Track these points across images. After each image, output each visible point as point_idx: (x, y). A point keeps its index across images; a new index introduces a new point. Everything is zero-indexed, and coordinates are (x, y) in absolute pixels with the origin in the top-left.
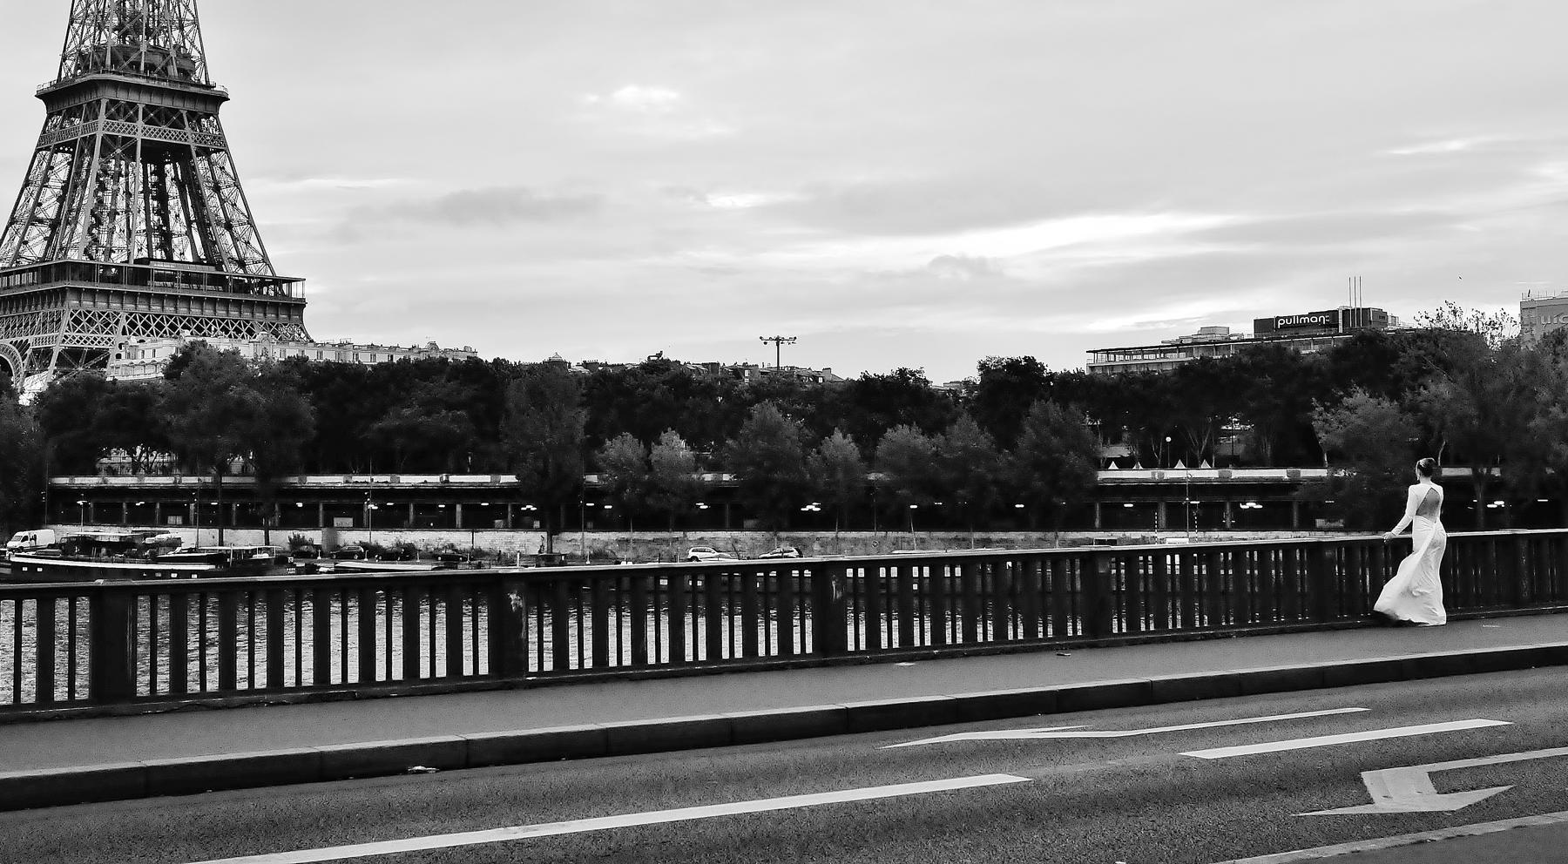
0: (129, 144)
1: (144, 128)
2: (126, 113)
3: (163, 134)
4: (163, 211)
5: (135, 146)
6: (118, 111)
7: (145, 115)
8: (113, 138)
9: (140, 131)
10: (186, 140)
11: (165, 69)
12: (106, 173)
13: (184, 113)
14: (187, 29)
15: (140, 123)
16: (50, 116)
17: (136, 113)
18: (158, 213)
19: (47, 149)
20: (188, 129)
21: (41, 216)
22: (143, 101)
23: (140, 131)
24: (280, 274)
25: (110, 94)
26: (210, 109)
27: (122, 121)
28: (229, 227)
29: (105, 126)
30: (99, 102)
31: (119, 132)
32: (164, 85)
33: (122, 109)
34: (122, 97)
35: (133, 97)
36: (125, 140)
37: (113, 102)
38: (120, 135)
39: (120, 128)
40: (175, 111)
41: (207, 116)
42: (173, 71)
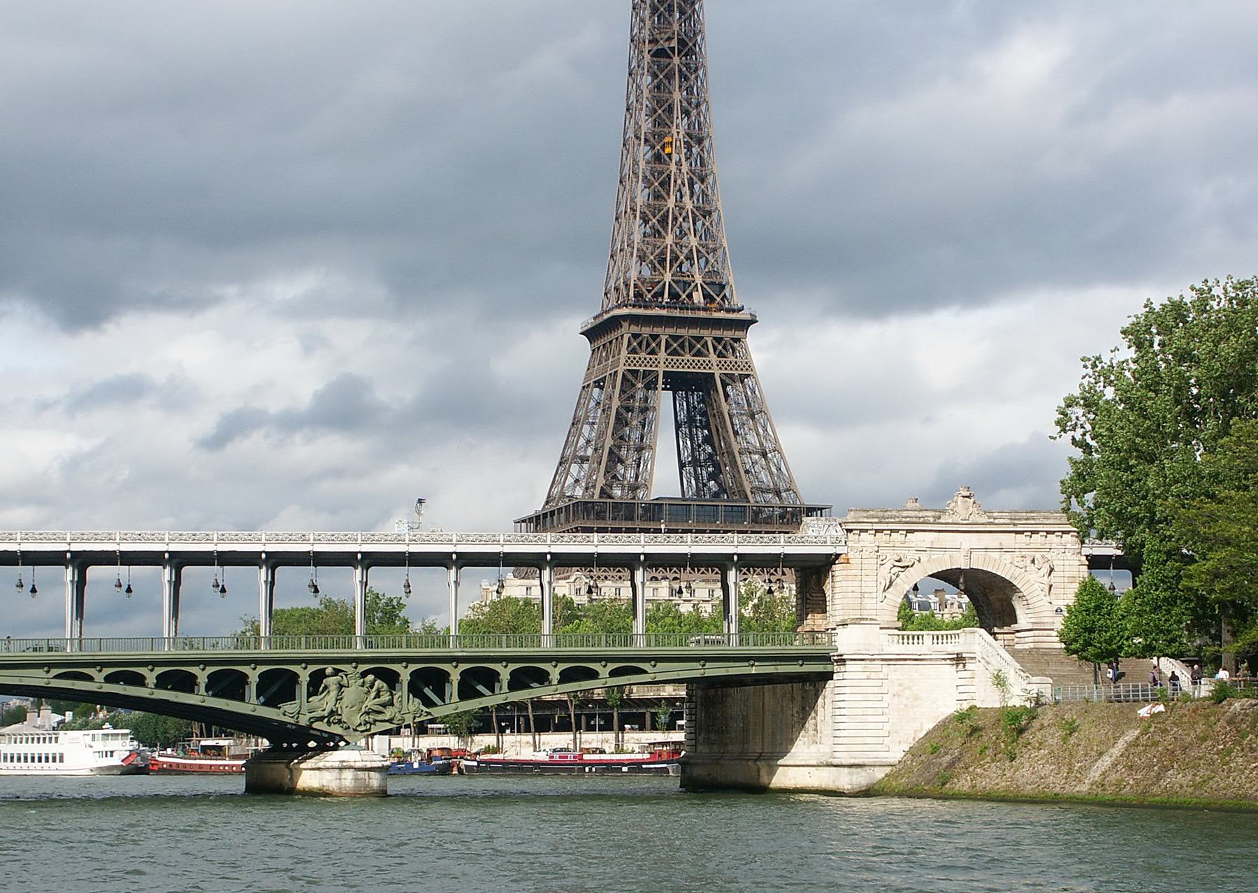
0: (650, 378)
1: (667, 360)
2: (648, 345)
3: (686, 364)
6: (640, 344)
7: (668, 346)
9: (662, 363)
10: (710, 368)
12: (628, 409)
15: (662, 355)
17: (659, 345)
20: (713, 357)
22: (664, 333)
23: (662, 363)
24: (809, 502)
26: (738, 334)
27: (643, 355)
29: (627, 361)
30: (622, 336)
31: (640, 365)
32: (690, 314)
33: (645, 343)
34: (646, 331)
35: (657, 331)
36: (646, 374)
37: (635, 336)
38: (642, 369)
39: (643, 362)
40: (699, 339)
41: (737, 340)
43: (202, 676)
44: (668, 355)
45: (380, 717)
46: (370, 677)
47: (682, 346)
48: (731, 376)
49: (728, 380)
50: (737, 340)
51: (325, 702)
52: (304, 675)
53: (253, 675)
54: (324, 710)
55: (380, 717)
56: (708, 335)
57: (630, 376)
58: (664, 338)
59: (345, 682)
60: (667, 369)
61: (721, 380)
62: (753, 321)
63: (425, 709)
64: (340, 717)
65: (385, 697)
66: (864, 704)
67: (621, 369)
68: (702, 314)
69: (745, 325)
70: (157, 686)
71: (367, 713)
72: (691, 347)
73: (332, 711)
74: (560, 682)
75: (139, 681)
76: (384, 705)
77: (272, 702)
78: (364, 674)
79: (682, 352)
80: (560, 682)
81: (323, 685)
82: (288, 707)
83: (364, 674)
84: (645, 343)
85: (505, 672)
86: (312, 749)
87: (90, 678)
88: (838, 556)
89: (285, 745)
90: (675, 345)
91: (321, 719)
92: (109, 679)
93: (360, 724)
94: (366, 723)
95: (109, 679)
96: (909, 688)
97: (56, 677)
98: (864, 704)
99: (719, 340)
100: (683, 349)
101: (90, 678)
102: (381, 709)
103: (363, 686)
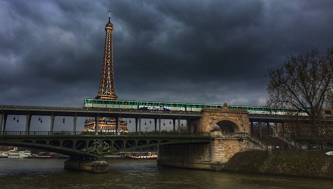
25: (102, 97)
32: (109, 96)
35: (105, 98)
42: (111, 94)
45: (107, 152)
52: (88, 142)
53: (75, 142)
55: (107, 152)
63: (117, 150)
65: (108, 147)
66: (219, 150)
68: (111, 96)
70: (49, 144)
71: (103, 151)
73: (95, 151)
74: (150, 143)
76: (108, 149)
77: (80, 148)
78: (103, 141)
80: (150, 143)
91: (92, 152)
92: (37, 142)
94: (103, 154)
96: (228, 146)
98: (219, 150)
101: (31, 142)
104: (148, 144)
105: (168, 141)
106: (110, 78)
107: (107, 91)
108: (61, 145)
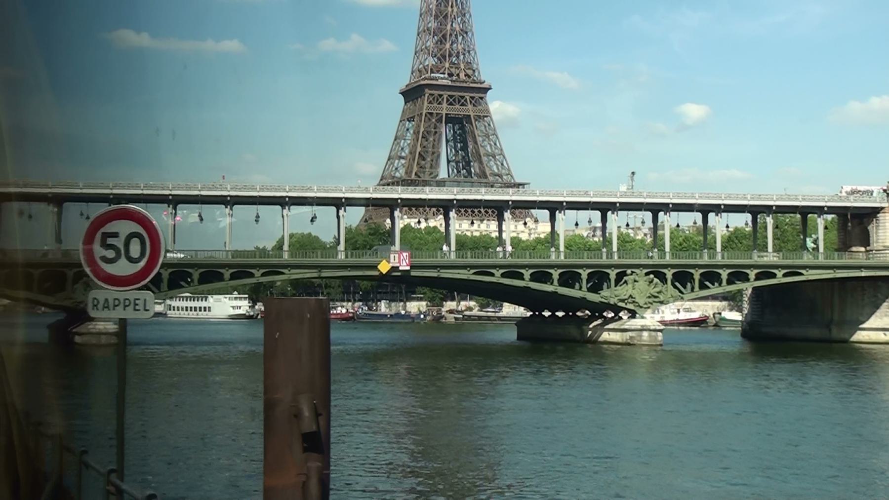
2: (438, 100)
3: (457, 110)
4: (465, 148)
5: (442, 116)
6: (434, 99)
7: (448, 100)
8: (431, 114)
11: (458, 75)
13: (468, 98)
14: (471, 52)
15: (445, 105)
16: (406, 103)
17: (443, 99)
18: (462, 149)
19: (404, 120)
20: (470, 107)
21: (403, 154)
22: (446, 94)
23: (444, 109)
24: (518, 181)
26: (482, 95)
27: (435, 105)
28: (494, 157)
33: (436, 99)
34: (436, 93)
39: (435, 108)
40: (463, 97)
42: (462, 76)
43: (556, 274)
44: (448, 105)
45: (656, 300)
46: (652, 276)
47: (454, 100)
48: (479, 117)
49: (479, 118)
50: (482, 98)
51: (623, 291)
52: (613, 274)
53: (584, 274)
54: (625, 295)
56: (467, 95)
57: (428, 115)
58: (445, 97)
59: (637, 279)
60: (447, 112)
61: (474, 118)
62: (490, 89)
64: (634, 300)
65: (657, 290)
67: (424, 112)
68: (464, 85)
69: (486, 90)
70: (531, 280)
71: (649, 297)
72: (459, 101)
75: (520, 277)
79: (454, 103)
81: (623, 281)
82: (605, 293)
83: (647, 274)
84: (436, 99)
85: (724, 274)
86: (597, 316)
87: (492, 275)
88: (883, 208)
89: (560, 314)
90: (451, 100)
91: (622, 301)
92: (503, 275)
93: (646, 304)
95: (503, 275)
97: (475, 274)
99: (472, 98)
100: (455, 102)
101: (492, 275)
102: (656, 294)
103: (646, 281)
104: (752, 280)
105: (801, 274)
106: (455, 9)
107: (447, 65)
108: (556, 282)
